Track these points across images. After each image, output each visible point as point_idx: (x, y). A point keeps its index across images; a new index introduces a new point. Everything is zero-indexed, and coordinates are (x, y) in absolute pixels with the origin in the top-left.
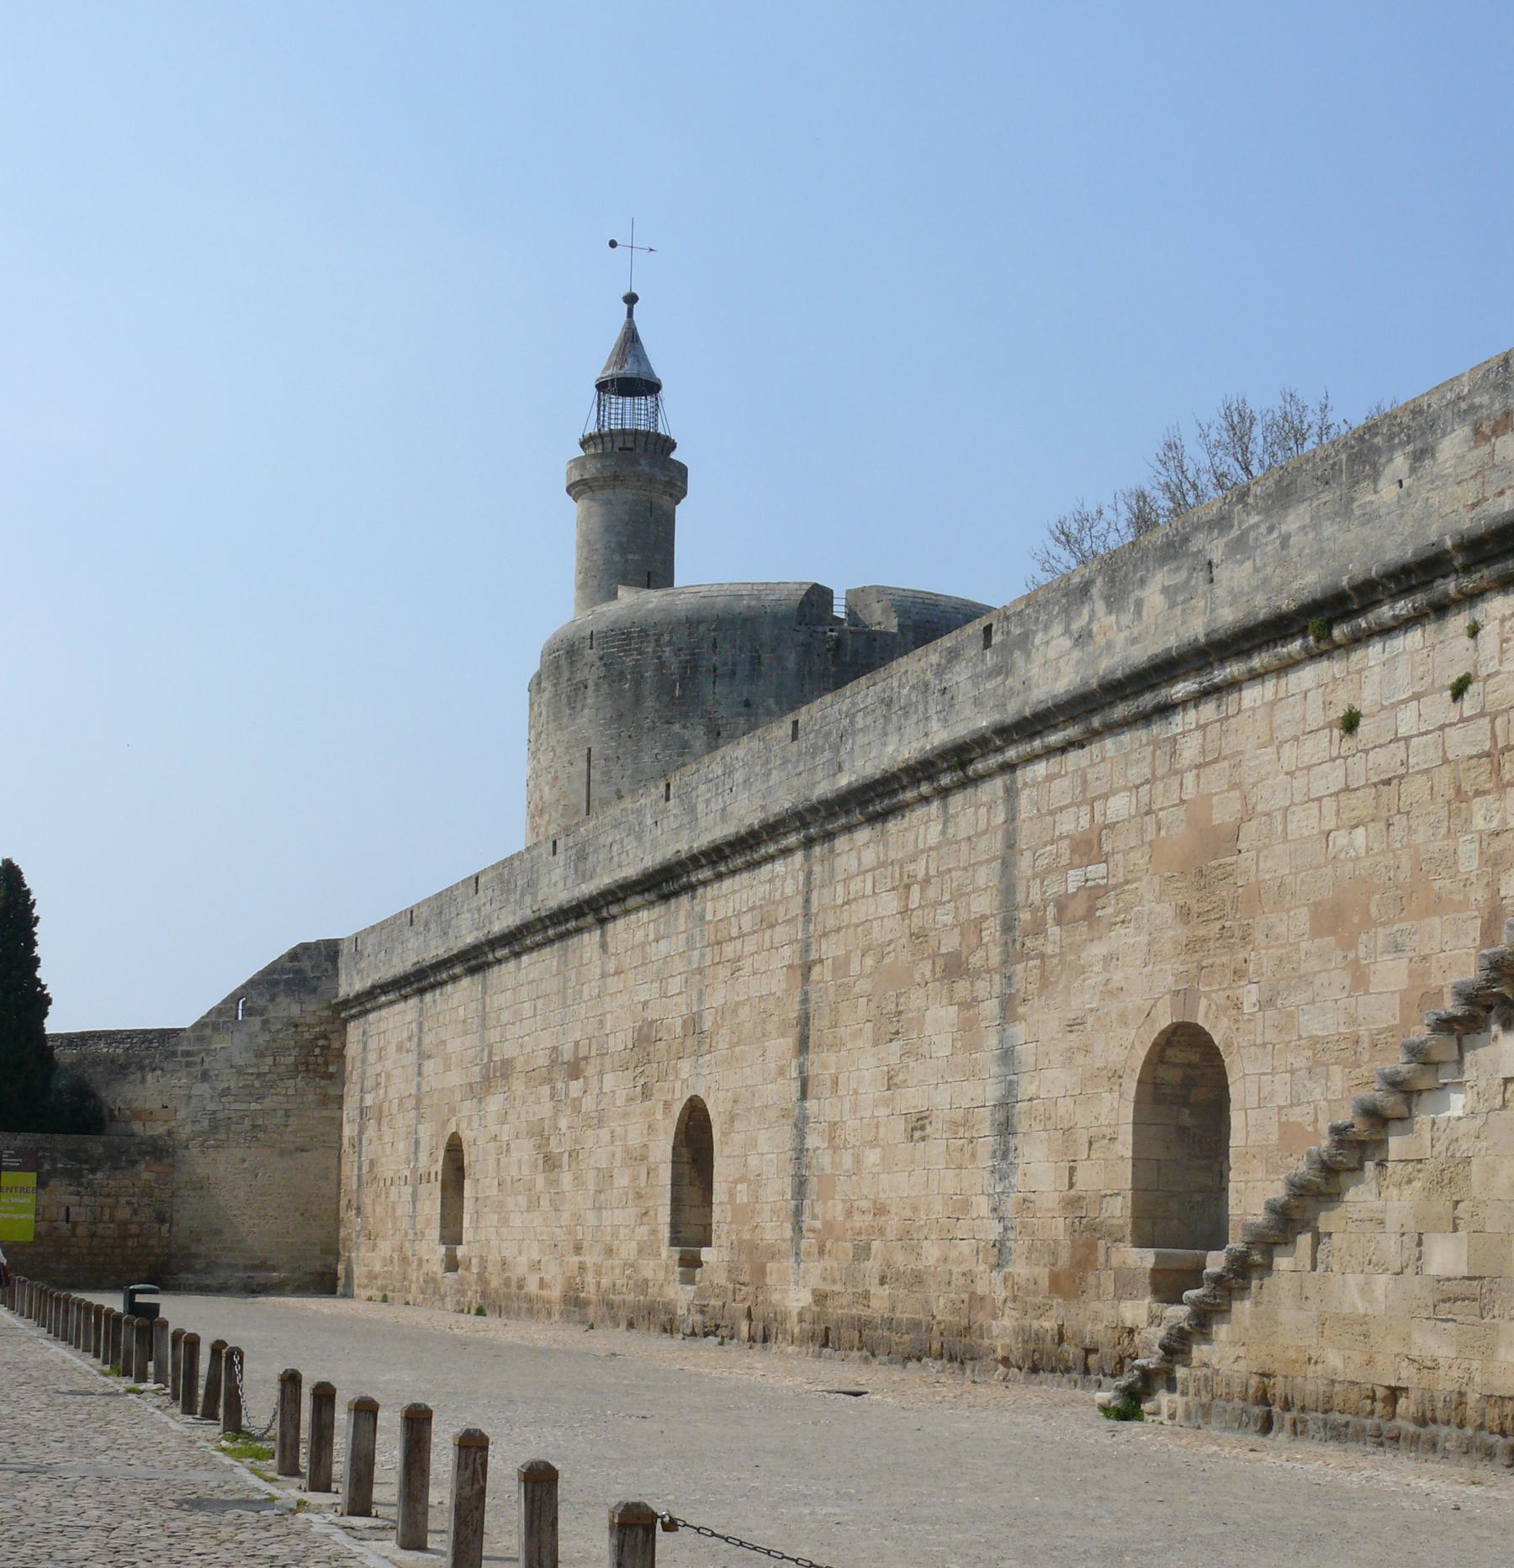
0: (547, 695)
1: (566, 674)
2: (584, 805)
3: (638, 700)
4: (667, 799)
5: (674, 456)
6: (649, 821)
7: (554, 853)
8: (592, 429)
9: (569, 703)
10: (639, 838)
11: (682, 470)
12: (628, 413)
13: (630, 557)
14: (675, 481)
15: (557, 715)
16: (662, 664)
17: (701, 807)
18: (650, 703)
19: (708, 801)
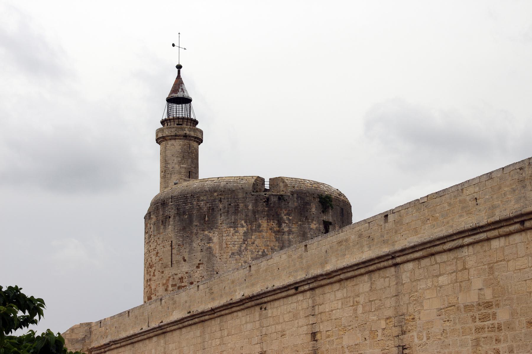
2: (170, 263)
5: (198, 126)
8: (165, 117)
12: (179, 110)
15: (158, 229)
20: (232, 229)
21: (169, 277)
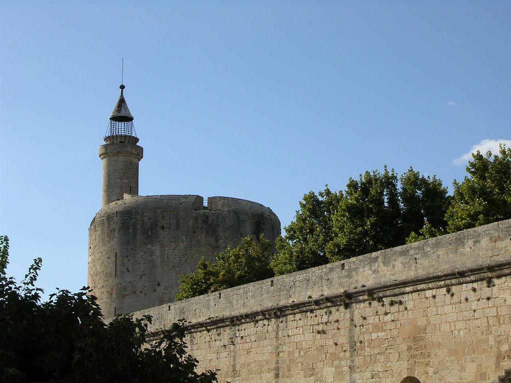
0: (98, 233)
1: (107, 225)
3: (135, 235)
4: (220, 298)
6: (212, 304)
7: (169, 310)
9: (108, 236)
10: (208, 308)
11: (141, 149)
12: (122, 128)
13: (124, 181)
14: (139, 153)
16: (144, 224)
17: (234, 302)
18: (139, 237)
19: (237, 301)
20: (173, 244)
21: (113, 286)
